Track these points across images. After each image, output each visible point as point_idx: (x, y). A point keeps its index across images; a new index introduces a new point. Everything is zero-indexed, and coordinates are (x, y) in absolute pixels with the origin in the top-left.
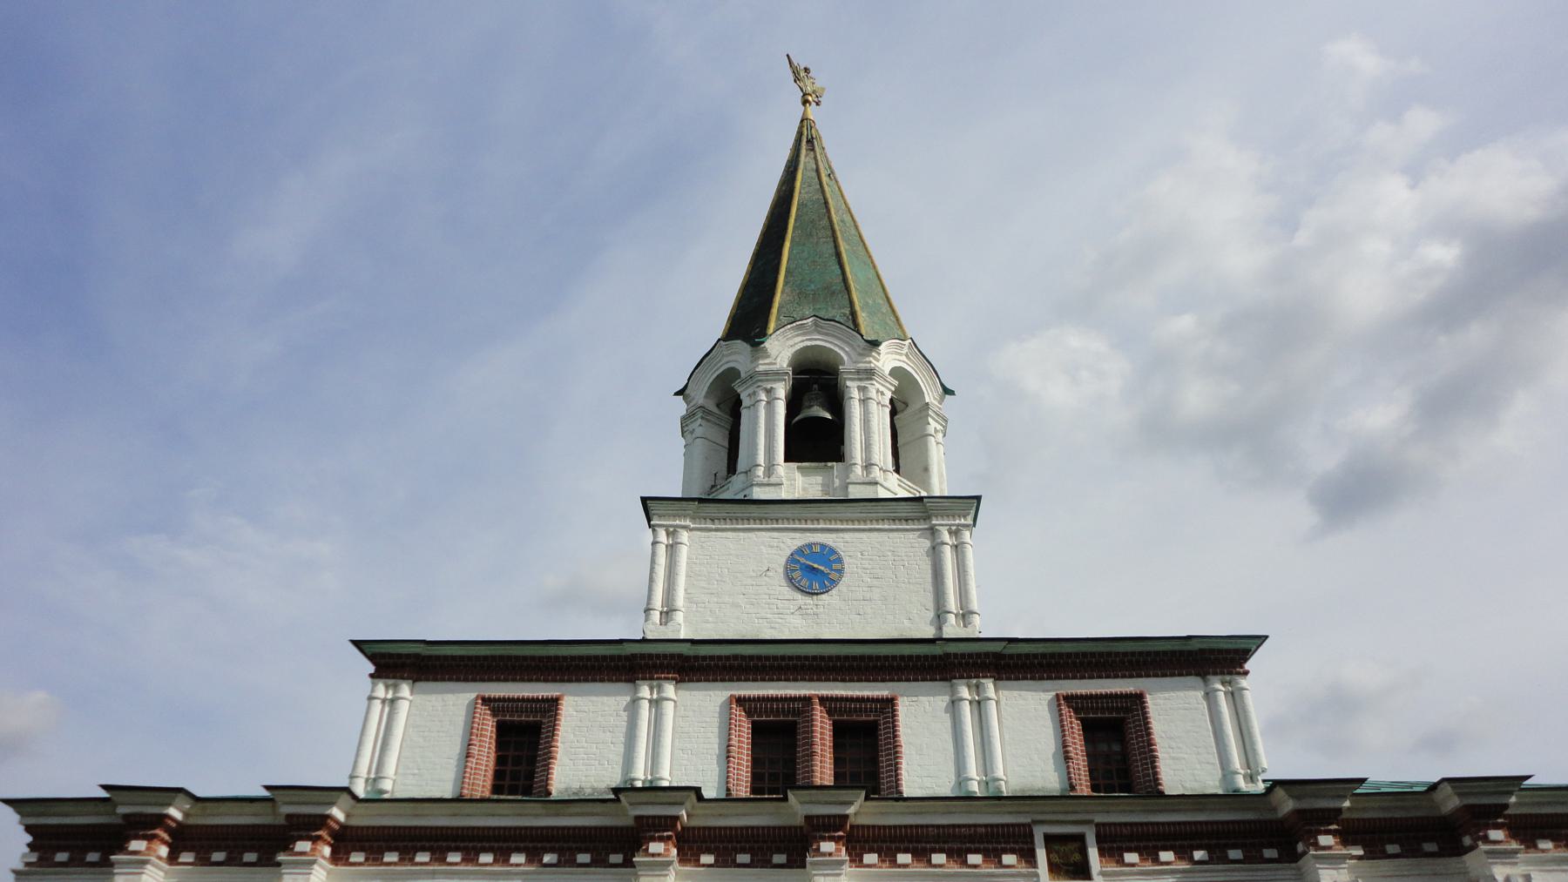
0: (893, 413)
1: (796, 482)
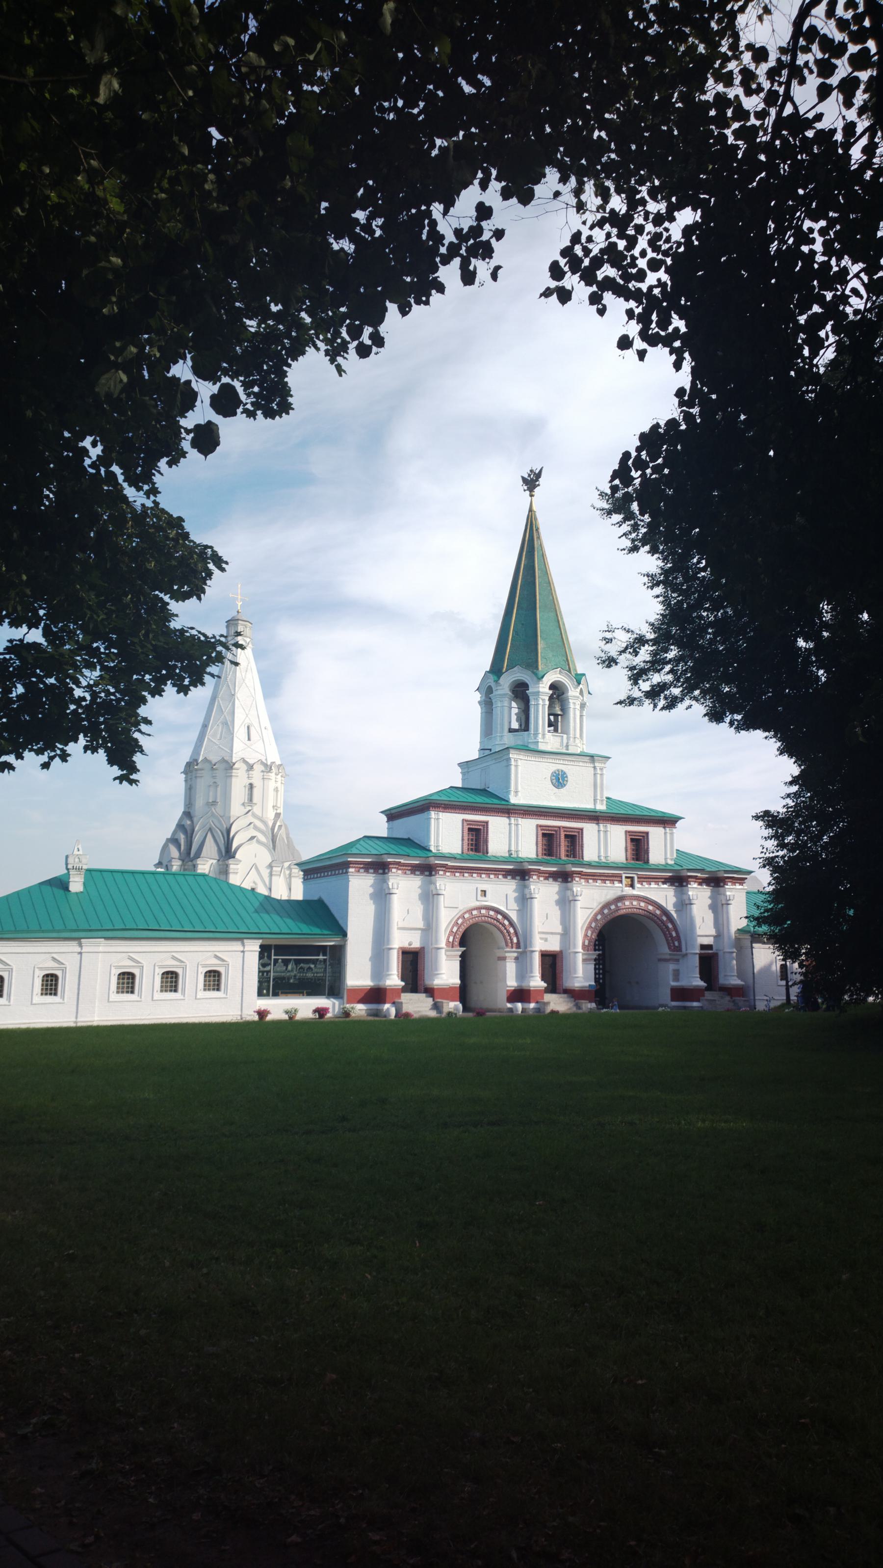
1: (549, 741)
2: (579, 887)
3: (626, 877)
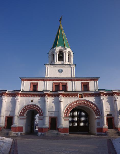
0: (68, 56)
1: (59, 63)
3: (79, 95)
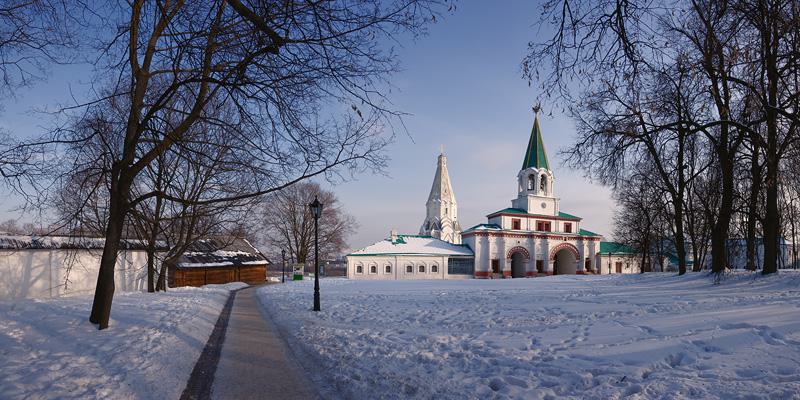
1: (541, 194)
2: (549, 240)
